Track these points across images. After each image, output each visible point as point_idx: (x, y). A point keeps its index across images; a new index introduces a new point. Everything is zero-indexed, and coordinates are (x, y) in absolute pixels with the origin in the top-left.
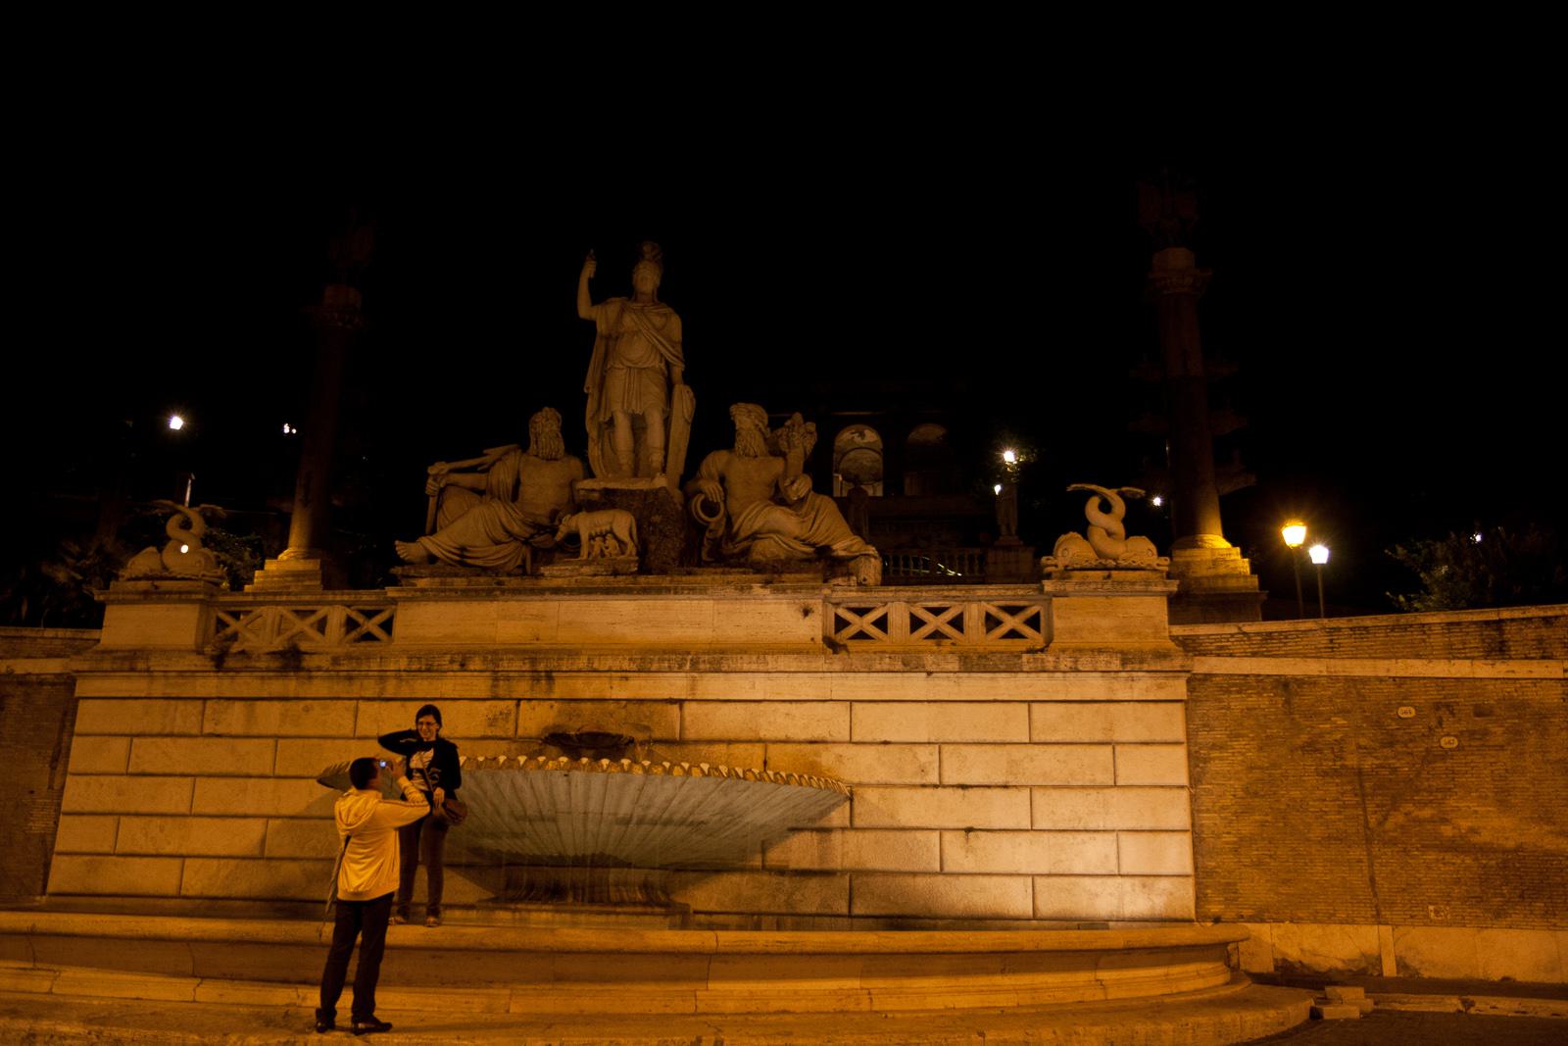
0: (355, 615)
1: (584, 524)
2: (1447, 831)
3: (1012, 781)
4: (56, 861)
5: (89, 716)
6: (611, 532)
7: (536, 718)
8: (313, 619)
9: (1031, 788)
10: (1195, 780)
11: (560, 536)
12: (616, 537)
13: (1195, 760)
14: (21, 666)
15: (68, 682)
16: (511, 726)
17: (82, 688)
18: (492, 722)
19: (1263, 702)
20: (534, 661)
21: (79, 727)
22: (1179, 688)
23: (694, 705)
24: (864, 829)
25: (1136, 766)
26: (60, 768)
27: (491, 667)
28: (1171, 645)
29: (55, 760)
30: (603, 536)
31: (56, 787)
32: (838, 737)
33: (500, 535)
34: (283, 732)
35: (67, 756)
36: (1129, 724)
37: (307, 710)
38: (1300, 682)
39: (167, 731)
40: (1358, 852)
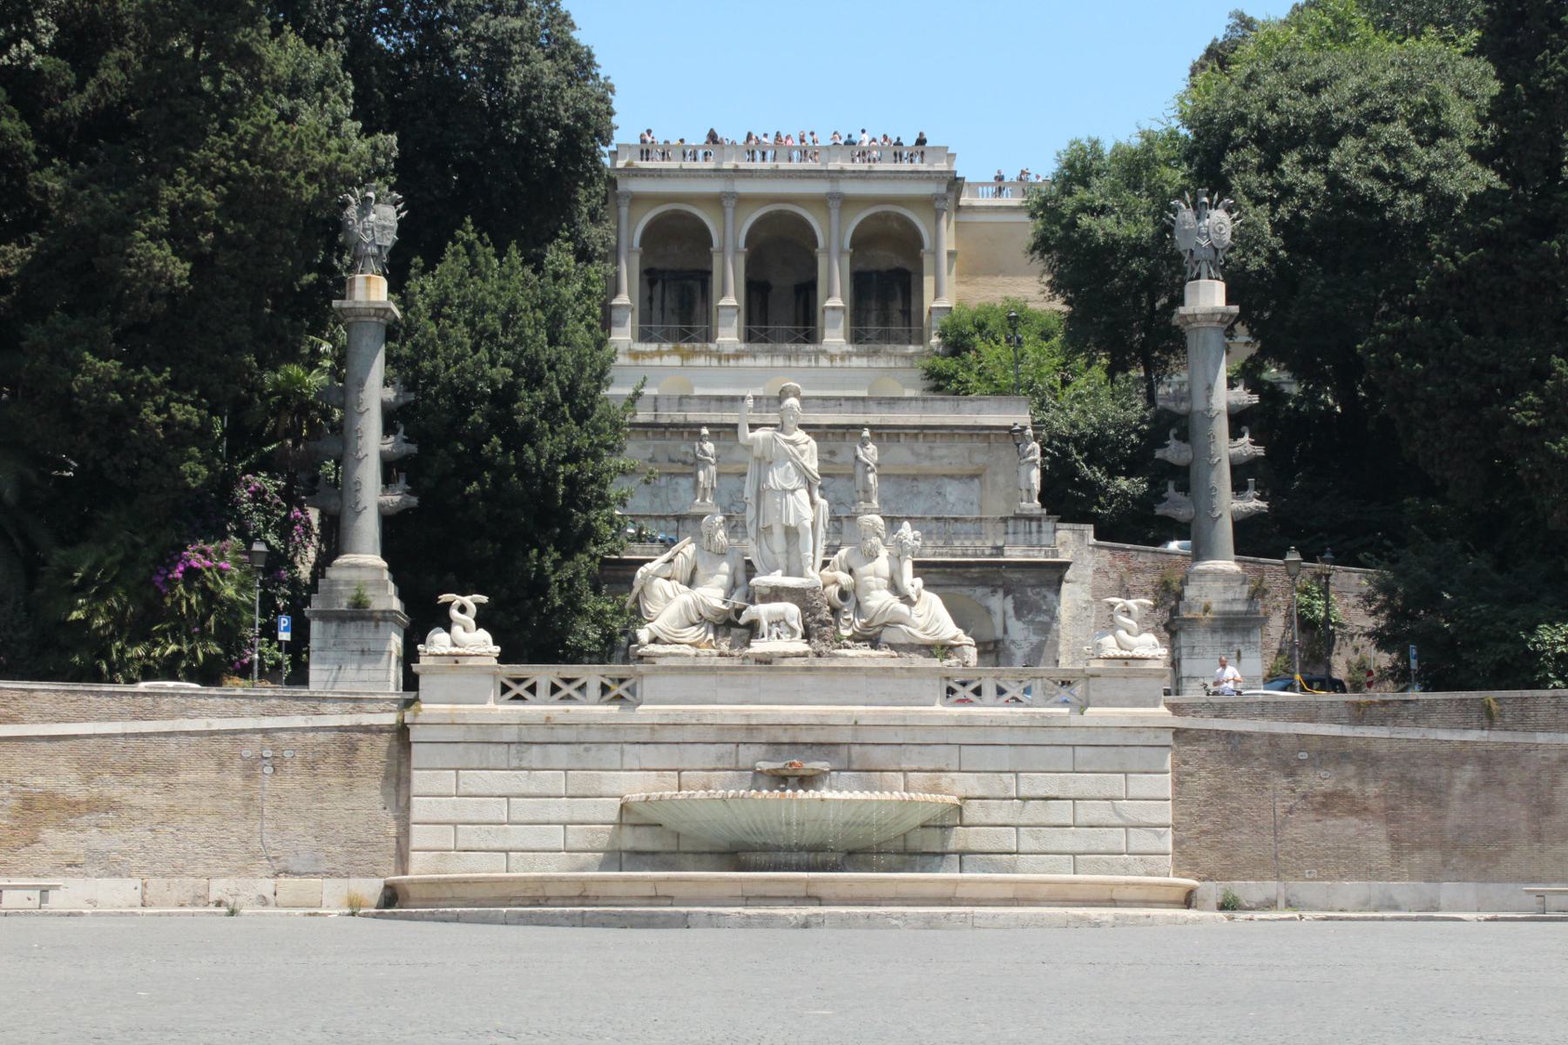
0: (607, 682)
3: (1061, 795)
4: (413, 855)
8: (577, 684)
11: (742, 621)
13: (1178, 783)
14: (366, 719)
16: (733, 761)
18: (719, 758)
21: (414, 763)
22: (1168, 738)
23: (858, 747)
26: (403, 792)
29: (398, 784)
30: (778, 623)
31: (402, 804)
33: (695, 618)
35: (408, 781)
37: (587, 750)
38: (1243, 736)
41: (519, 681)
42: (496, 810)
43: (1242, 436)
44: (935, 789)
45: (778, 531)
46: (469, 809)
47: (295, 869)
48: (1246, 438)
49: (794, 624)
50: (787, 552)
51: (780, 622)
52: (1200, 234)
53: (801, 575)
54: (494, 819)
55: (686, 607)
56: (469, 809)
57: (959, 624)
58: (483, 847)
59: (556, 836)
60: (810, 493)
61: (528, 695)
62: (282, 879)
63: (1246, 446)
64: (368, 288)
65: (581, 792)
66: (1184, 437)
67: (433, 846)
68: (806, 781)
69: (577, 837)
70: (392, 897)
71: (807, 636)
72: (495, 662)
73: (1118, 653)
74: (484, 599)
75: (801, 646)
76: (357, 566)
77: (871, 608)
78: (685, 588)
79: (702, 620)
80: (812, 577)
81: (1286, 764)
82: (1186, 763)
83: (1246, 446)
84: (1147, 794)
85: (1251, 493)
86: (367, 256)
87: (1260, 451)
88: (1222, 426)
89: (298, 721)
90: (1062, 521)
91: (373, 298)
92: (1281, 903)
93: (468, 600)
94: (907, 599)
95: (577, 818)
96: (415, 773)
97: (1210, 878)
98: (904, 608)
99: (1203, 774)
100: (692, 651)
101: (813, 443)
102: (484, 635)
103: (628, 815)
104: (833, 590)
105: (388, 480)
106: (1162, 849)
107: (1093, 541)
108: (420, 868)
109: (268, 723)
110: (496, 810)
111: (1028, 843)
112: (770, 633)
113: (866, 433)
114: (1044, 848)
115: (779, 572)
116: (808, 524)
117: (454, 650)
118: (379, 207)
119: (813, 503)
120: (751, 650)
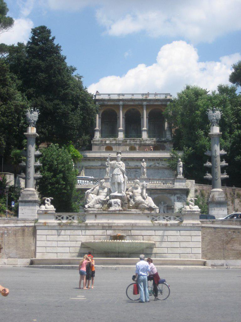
1: (113, 201)
2: (233, 248)
3: (177, 241)
5: (39, 232)
6: (117, 203)
7: (110, 232)
9: (180, 242)
10: (203, 241)
12: (118, 204)
13: (203, 238)
14: (27, 225)
15: (35, 227)
17: (37, 228)
18: (103, 233)
19: (212, 230)
20: (109, 224)
24: (157, 248)
25: (194, 239)
27: (102, 225)
28: (200, 222)
32: (153, 235)
34: (70, 234)
36: (194, 233)
39: (52, 234)
40: (222, 251)
41: (60, 216)
42: (54, 244)
43: (223, 161)
44: (149, 240)
45: (116, 183)
46: (49, 244)
47: (13, 257)
48: (224, 162)
49: (119, 204)
50: (118, 188)
51: (116, 203)
52: (213, 116)
53: (121, 193)
54: (54, 246)
55: (96, 200)
56: (49, 244)
57: (155, 203)
58: (52, 252)
59: (67, 250)
60: (123, 175)
61: (62, 219)
62: (9, 259)
63: (224, 163)
64: (32, 130)
65: (73, 240)
66: (210, 161)
67: (41, 252)
68: (121, 238)
69: (72, 250)
70: (32, 263)
71: (122, 206)
72: (54, 212)
73: (189, 210)
74: (53, 198)
75: (121, 209)
76: (29, 191)
77: (136, 200)
78: (96, 196)
79: (100, 203)
80: (124, 193)
81: (226, 234)
82: (204, 234)
83: (224, 163)
84: (196, 241)
85: (225, 173)
86: (31, 123)
87: (227, 164)
88: (218, 159)
89: (12, 225)
90: (187, 179)
91: (33, 132)
92: (225, 265)
93: (49, 199)
94: (144, 198)
95: (71, 246)
96: (37, 236)
97: (209, 259)
98: (143, 200)
99: (208, 236)
100: (97, 210)
101: (124, 164)
102: (52, 206)
103: (83, 246)
104: (128, 196)
105: (36, 171)
106: (199, 253)
107: (194, 184)
108: (39, 256)
109: (6, 225)
110: (54, 244)
111: (170, 251)
112: (114, 206)
113: (144, 160)
114: (174, 253)
115: (117, 192)
116: (123, 182)
117: (46, 209)
118: (34, 112)
119: (124, 177)
120: (110, 210)
